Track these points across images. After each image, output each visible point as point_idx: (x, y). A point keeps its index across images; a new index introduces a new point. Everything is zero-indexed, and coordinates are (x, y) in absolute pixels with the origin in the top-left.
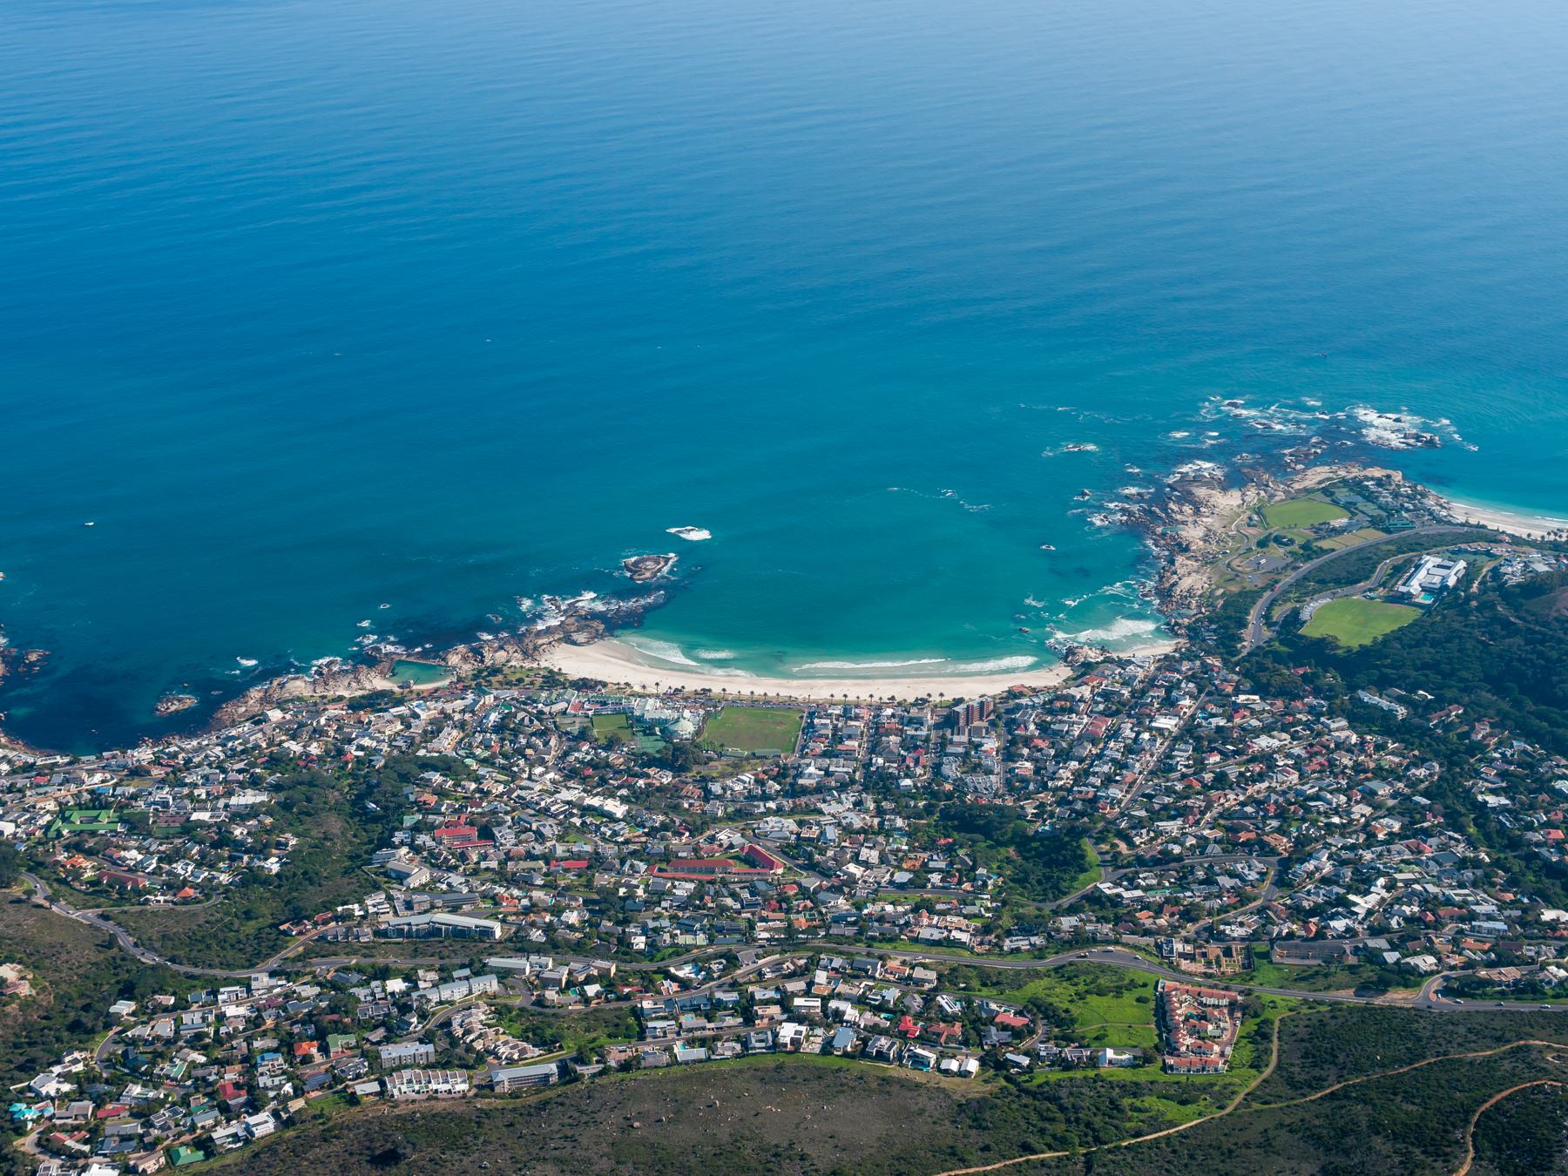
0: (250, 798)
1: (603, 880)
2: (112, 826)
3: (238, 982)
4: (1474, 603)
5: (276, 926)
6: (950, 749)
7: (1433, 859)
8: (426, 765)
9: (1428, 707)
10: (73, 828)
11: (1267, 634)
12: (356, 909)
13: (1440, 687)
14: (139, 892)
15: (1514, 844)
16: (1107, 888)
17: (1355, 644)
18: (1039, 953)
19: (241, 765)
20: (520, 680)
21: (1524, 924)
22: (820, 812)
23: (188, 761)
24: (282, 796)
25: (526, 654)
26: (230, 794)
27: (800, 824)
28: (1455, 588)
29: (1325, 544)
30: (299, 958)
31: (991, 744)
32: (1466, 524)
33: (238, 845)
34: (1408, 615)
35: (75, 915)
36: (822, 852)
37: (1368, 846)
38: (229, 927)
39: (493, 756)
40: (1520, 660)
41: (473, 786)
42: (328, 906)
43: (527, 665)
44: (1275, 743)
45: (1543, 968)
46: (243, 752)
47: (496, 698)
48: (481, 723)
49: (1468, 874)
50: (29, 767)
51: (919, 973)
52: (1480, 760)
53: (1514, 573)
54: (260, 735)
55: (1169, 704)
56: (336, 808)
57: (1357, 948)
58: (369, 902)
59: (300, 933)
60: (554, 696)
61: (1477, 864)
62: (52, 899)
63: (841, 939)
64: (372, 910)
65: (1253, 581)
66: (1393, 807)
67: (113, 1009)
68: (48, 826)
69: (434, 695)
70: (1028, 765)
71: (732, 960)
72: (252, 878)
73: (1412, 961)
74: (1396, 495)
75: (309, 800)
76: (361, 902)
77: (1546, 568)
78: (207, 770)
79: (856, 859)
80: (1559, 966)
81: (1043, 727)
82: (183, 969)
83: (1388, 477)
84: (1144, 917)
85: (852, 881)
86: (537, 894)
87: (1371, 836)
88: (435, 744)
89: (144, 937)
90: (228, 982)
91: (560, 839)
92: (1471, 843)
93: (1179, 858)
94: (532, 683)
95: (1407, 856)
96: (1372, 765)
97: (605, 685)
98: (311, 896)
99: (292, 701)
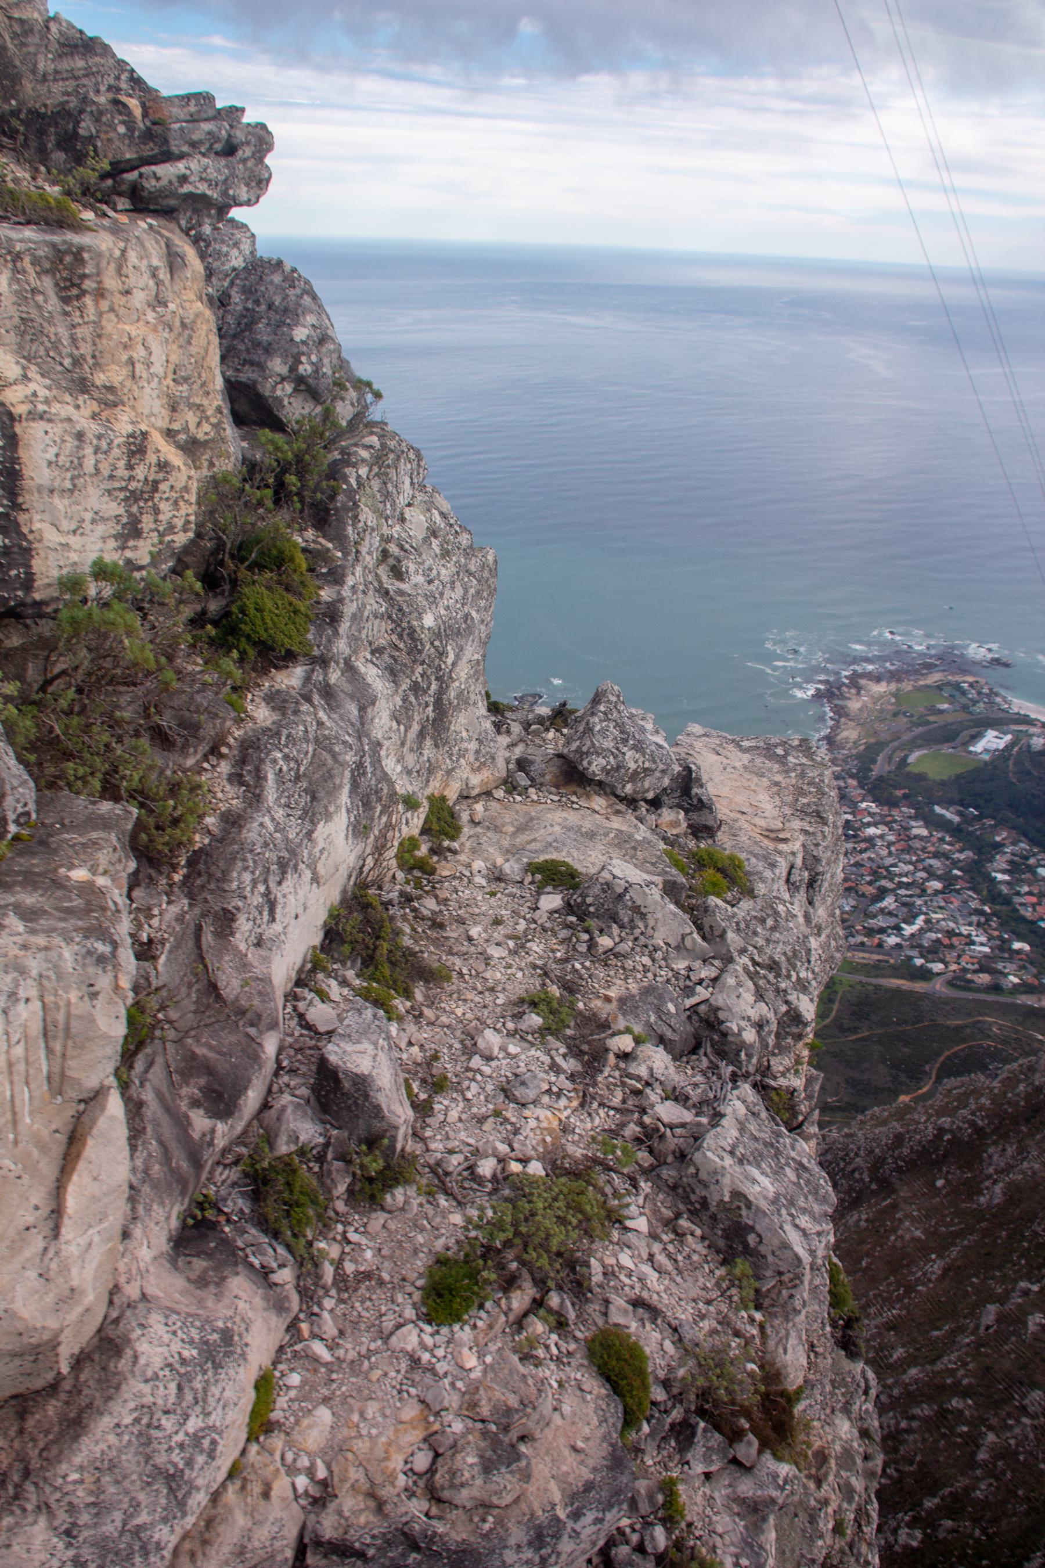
11: (887, 768)
17: (938, 778)
21: (1001, 949)
29: (931, 718)
44: (878, 832)
45: (1005, 975)
49: (975, 919)
61: (979, 912)
65: (884, 736)
74: (979, 693)
87: (924, 891)
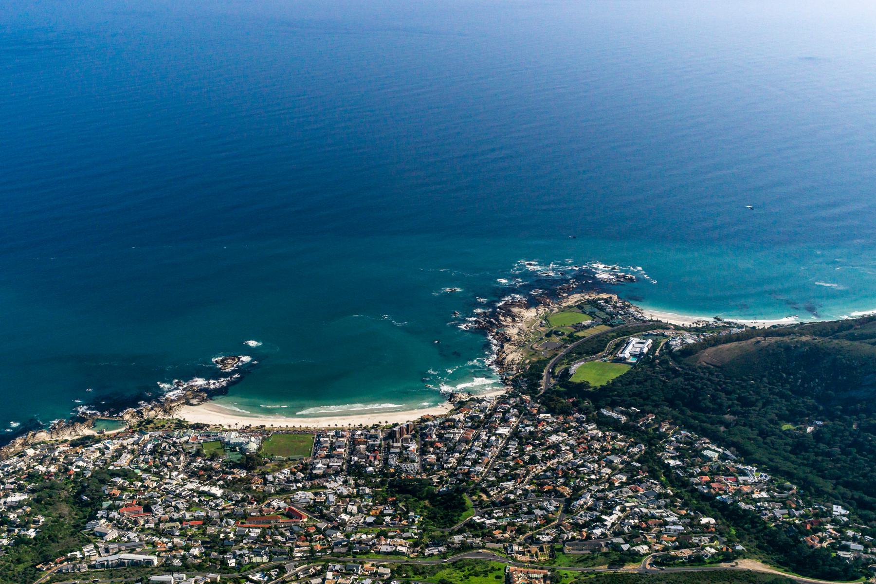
1: (211, 530)
4: (658, 361)
5: (34, 566)
6: (392, 450)
7: (644, 494)
8: (114, 474)
9: (637, 416)
12: (78, 554)
13: (643, 405)
15: (685, 484)
16: (477, 519)
17: (598, 385)
18: (443, 555)
19: (12, 480)
20: (163, 426)
22: (326, 488)
24: (35, 495)
25: (166, 412)
26: (6, 496)
27: (316, 494)
28: (647, 353)
29: (580, 334)
31: (413, 447)
32: (651, 320)
33: (12, 523)
34: (624, 369)
36: (327, 508)
37: (610, 490)
39: (150, 467)
40: (683, 389)
41: (140, 484)
42: (62, 554)
43: (167, 417)
44: (560, 438)
45: (703, 548)
46: (13, 473)
48: (142, 450)
49: (662, 502)
51: (381, 570)
52: (665, 442)
53: (676, 344)
55: (505, 421)
56: (66, 500)
57: (608, 543)
58: (85, 550)
59: (48, 569)
61: (666, 496)
63: (339, 554)
64: (86, 554)
66: (622, 469)
69: (116, 437)
70: (433, 456)
71: (282, 570)
72: (20, 541)
73: (636, 548)
74: (615, 307)
75: (50, 496)
76: (81, 550)
77: (693, 341)
79: (345, 511)
80: (711, 547)
81: (440, 436)
83: (611, 298)
84: (497, 534)
85: (344, 523)
86: (176, 540)
87: (612, 484)
88: (118, 462)
91: (188, 509)
92: (663, 485)
93: (514, 501)
94: (169, 427)
95: (631, 494)
96: (610, 447)
97: (208, 426)
98: (53, 548)
99: (39, 443)
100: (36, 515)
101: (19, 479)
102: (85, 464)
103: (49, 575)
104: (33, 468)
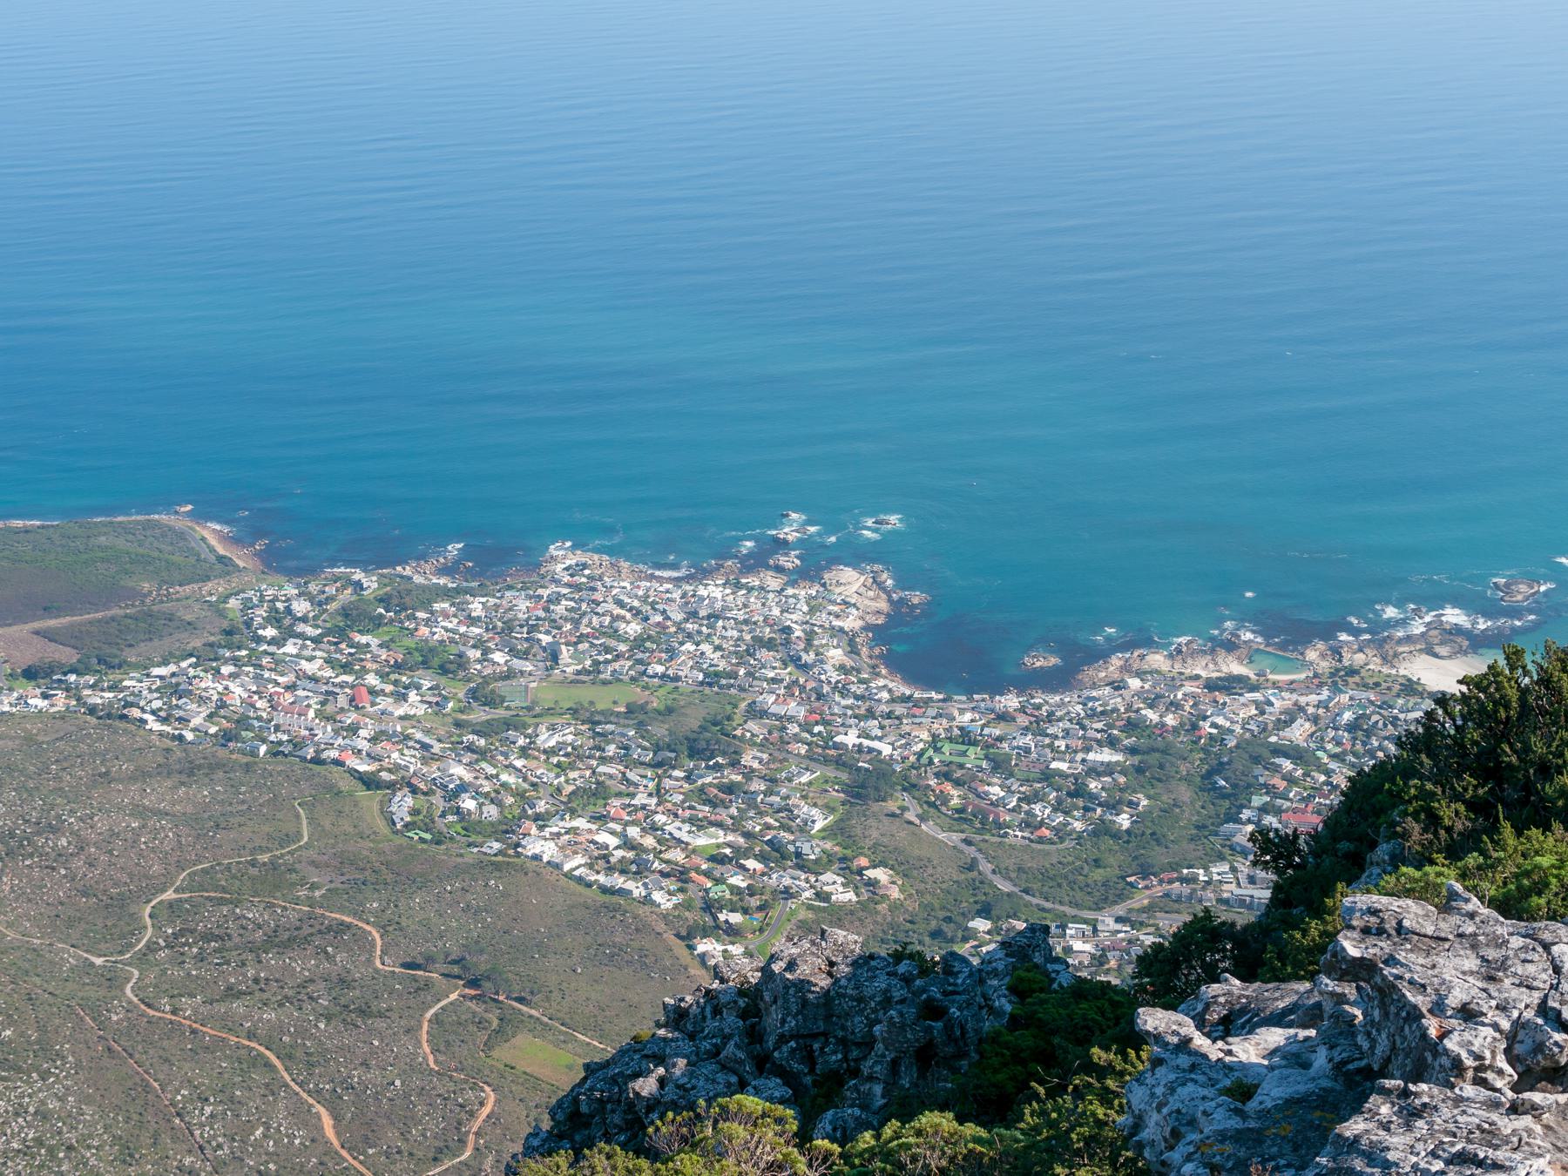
0: (1106, 756)
2: (978, 762)
3: (1085, 922)
5: (1124, 878)
8: (1278, 751)
10: (943, 758)
14: (1000, 826)
19: (1099, 726)
20: (1377, 684)
23: (1050, 714)
24: (1136, 759)
25: (1385, 660)
26: (1088, 750)
30: (1143, 910)
33: (1092, 797)
35: (942, 836)
38: (1079, 871)
39: (1344, 753)
41: (1323, 778)
42: (1175, 867)
43: (1385, 670)
46: (1103, 713)
47: (1351, 699)
48: (1334, 721)
50: (906, 699)
54: (1119, 700)
56: (1187, 779)
59: (1147, 887)
60: (1410, 704)
62: (922, 818)
64: (1216, 877)
67: (971, 924)
68: (920, 754)
69: (1291, 687)
72: (1103, 830)
75: (1161, 767)
76: (1206, 869)
78: (1068, 725)
82: (1035, 901)
89: (1003, 866)
90: (1076, 919)
94: (1389, 689)
98: (1158, 856)
99: (1150, 673)
100: (1135, 791)
101: (1110, 726)
102: (1228, 724)
103: (1149, 897)
104: (1137, 711)
